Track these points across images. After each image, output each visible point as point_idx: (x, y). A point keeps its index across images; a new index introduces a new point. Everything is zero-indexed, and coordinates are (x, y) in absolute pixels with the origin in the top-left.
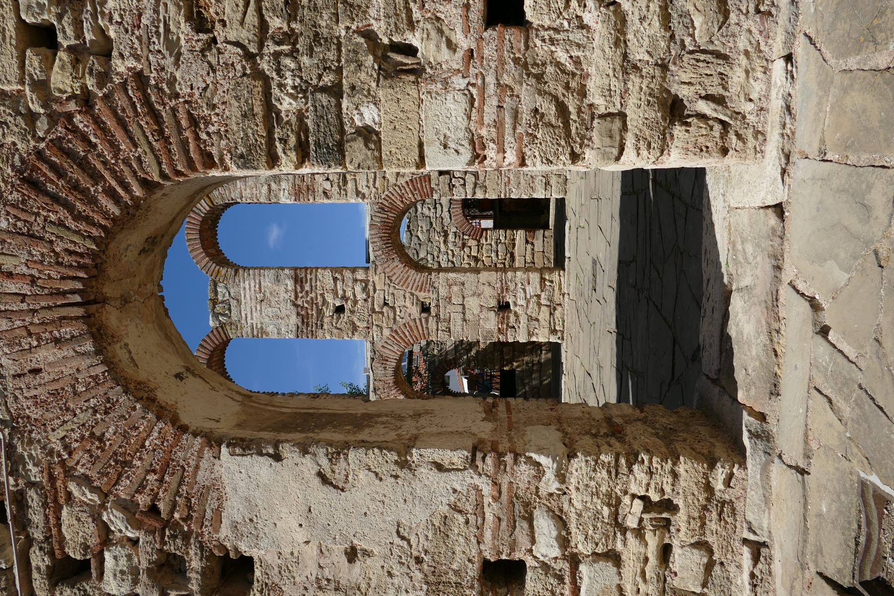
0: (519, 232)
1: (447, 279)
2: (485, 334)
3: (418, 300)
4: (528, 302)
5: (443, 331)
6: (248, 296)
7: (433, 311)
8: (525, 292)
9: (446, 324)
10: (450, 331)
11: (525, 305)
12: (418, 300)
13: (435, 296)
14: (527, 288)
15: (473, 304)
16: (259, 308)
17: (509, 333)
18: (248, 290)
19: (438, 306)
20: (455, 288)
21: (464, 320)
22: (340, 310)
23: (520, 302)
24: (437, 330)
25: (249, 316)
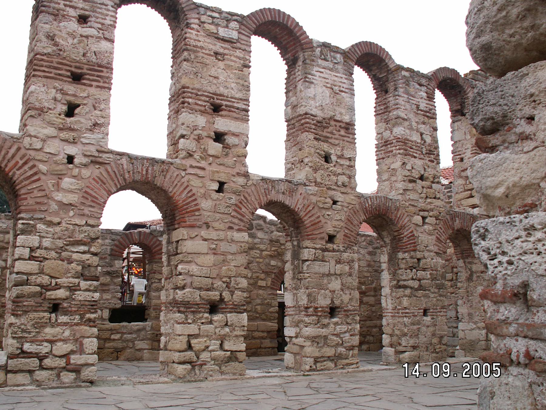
0: (276, 325)
1: (353, 261)
2: (314, 294)
3: (338, 232)
4: (337, 335)
5: (315, 254)
6: (336, 79)
7: (330, 246)
8: (345, 332)
9: (320, 257)
10: (314, 260)
11: (336, 333)
12: (338, 232)
13: (342, 249)
14: (347, 334)
15: (336, 285)
16: (329, 85)
17: (314, 318)
18: (340, 80)
19: (334, 251)
20: (347, 268)
21: (324, 275)
22: (327, 158)
23: (338, 328)
24: (315, 249)
25: (321, 75)
